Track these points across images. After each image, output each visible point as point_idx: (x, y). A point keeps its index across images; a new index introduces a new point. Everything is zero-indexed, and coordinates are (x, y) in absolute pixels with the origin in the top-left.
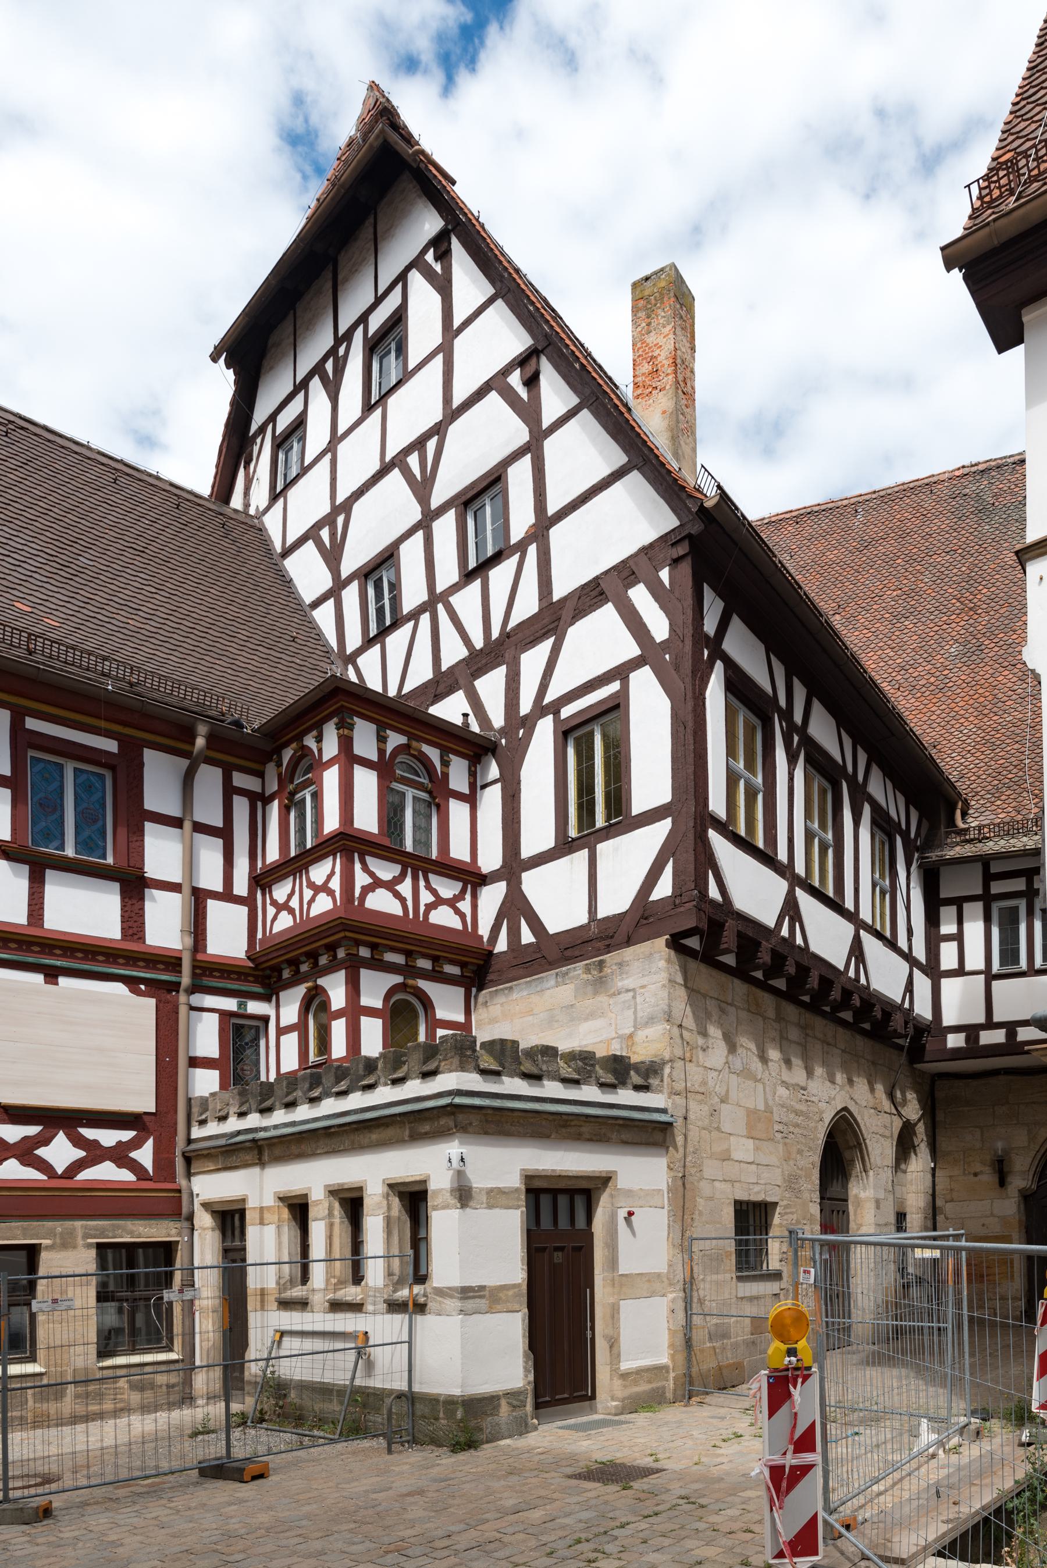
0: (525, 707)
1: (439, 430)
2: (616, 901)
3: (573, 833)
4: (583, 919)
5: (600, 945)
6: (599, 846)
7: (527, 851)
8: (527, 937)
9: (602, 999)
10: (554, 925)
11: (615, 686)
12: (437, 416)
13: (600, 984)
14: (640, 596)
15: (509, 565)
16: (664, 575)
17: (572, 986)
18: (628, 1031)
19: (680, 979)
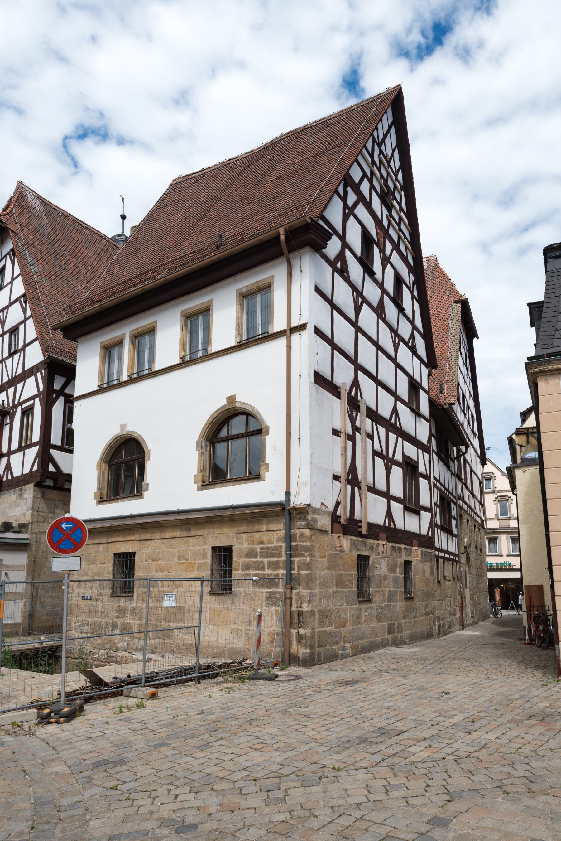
0: (16, 403)
1: (7, 308)
2: (26, 471)
3: (23, 445)
4: (20, 474)
5: (23, 482)
6: (26, 451)
7: (12, 449)
8: (10, 477)
9: (21, 500)
10: (15, 475)
11: (32, 402)
12: (7, 304)
13: (21, 495)
14: (39, 375)
15: (18, 355)
16: (43, 371)
17: (15, 495)
18: (24, 512)
19: (40, 496)
